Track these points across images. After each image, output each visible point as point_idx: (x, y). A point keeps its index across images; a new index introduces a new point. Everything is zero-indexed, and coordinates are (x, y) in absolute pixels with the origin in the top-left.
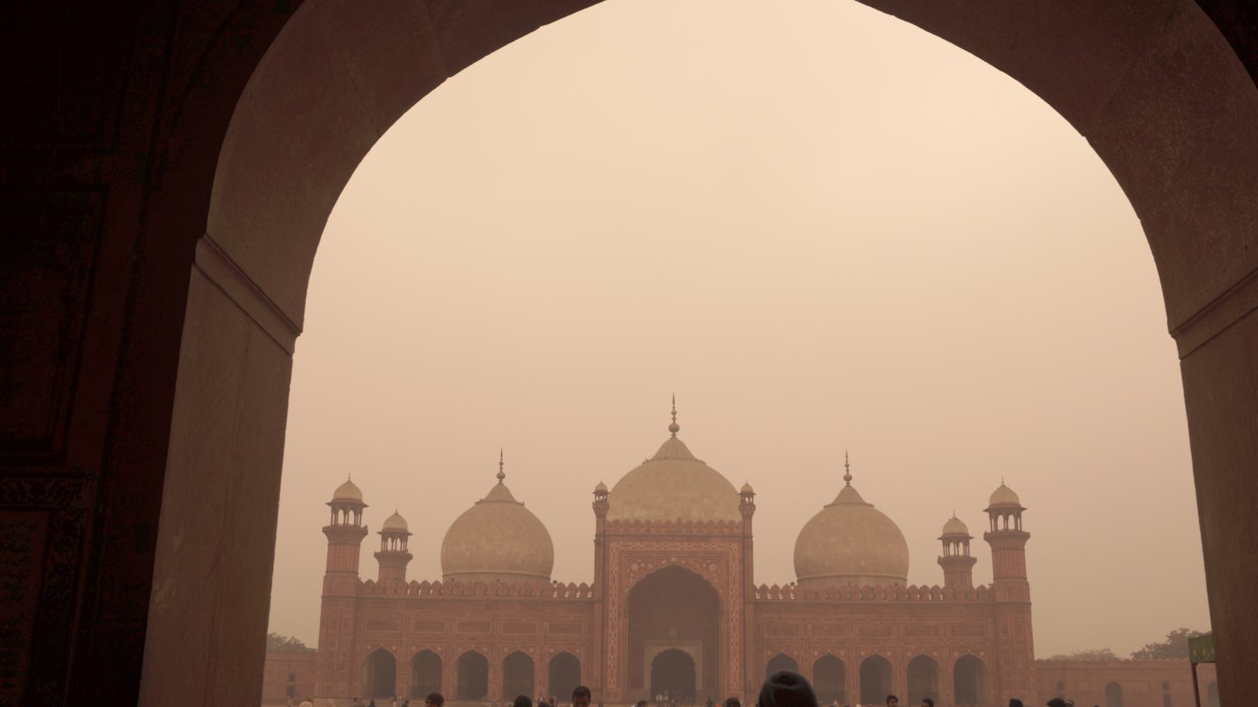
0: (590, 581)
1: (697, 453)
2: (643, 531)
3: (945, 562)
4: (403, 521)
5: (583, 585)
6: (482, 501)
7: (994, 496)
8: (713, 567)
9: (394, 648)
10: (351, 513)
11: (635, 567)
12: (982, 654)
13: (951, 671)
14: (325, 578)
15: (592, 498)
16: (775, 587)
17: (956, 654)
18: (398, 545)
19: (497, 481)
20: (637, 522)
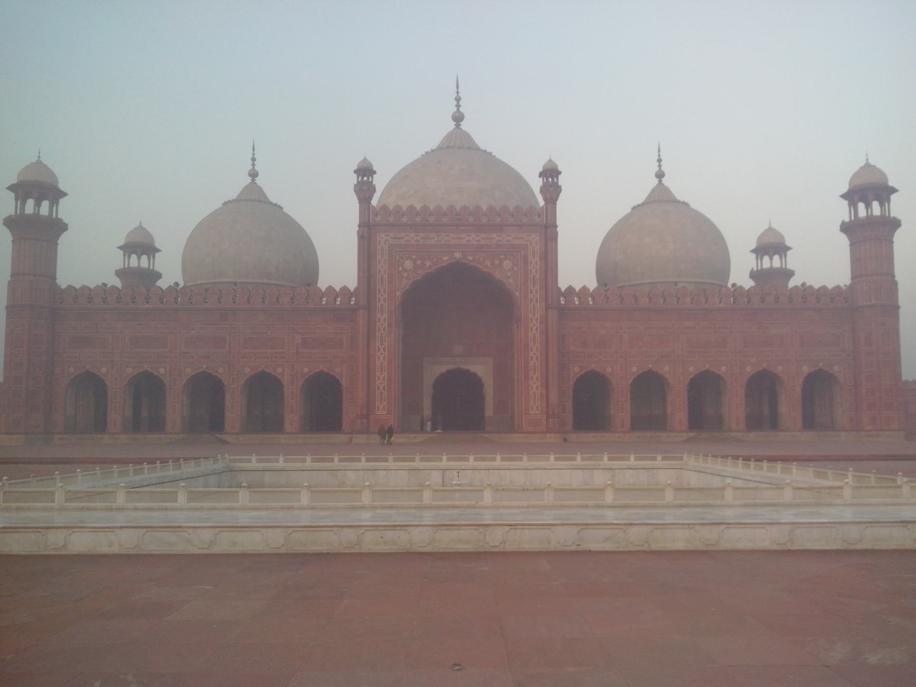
0: (352, 285)
1: (483, 147)
2: (418, 219)
3: (754, 275)
4: (148, 234)
5: (345, 289)
6: (229, 202)
7: (856, 175)
8: (507, 264)
9: (104, 370)
10: (45, 204)
11: (408, 264)
12: (836, 368)
13: (798, 389)
14: (9, 283)
15: (354, 179)
16: (584, 289)
17: (806, 369)
18: (144, 262)
19: (249, 180)
20: (411, 208)
